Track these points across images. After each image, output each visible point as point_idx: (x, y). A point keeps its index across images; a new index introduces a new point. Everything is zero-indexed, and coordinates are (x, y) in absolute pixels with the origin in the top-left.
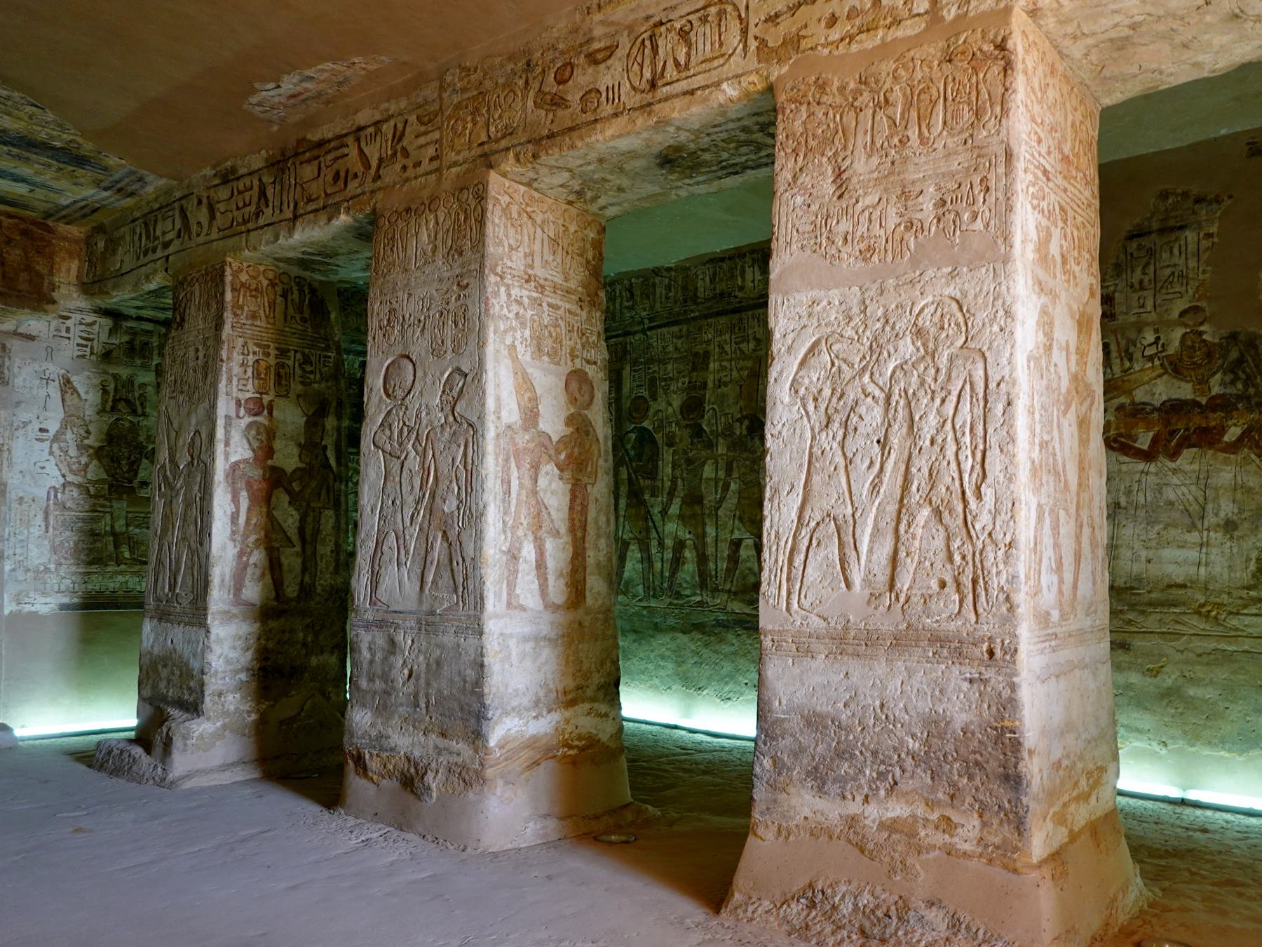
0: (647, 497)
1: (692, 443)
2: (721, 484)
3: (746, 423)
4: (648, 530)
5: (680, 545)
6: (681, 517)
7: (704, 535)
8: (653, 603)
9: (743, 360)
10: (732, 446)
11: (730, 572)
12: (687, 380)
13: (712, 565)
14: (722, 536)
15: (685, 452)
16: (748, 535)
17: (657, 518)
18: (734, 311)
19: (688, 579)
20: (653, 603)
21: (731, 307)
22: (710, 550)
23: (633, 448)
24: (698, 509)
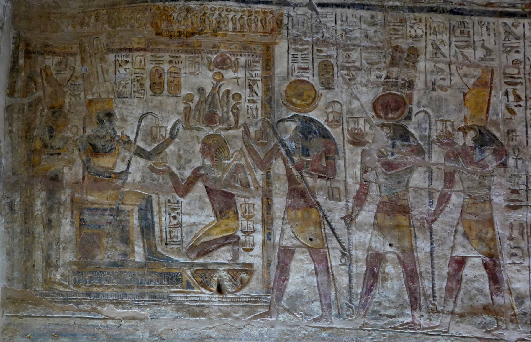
0: (321, 198)
1: (394, 146)
2: (437, 196)
3: (472, 134)
4: (324, 239)
5: (375, 260)
6: (378, 226)
7: (412, 249)
8: (337, 324)
9: (468, 66)
10: (454, 155)
11: (451, 292)
12: (384, 74)
13: (427, 284)
14: (438, 251)
15: (381, 155)
16: (476, 253)
17: (340, 226)
18: (453, 12)
19: (392, 297)
20: (337, 324)
21: (449, 7)
22: (423, 267)
23: (291, 139)
24: (402, 219)
